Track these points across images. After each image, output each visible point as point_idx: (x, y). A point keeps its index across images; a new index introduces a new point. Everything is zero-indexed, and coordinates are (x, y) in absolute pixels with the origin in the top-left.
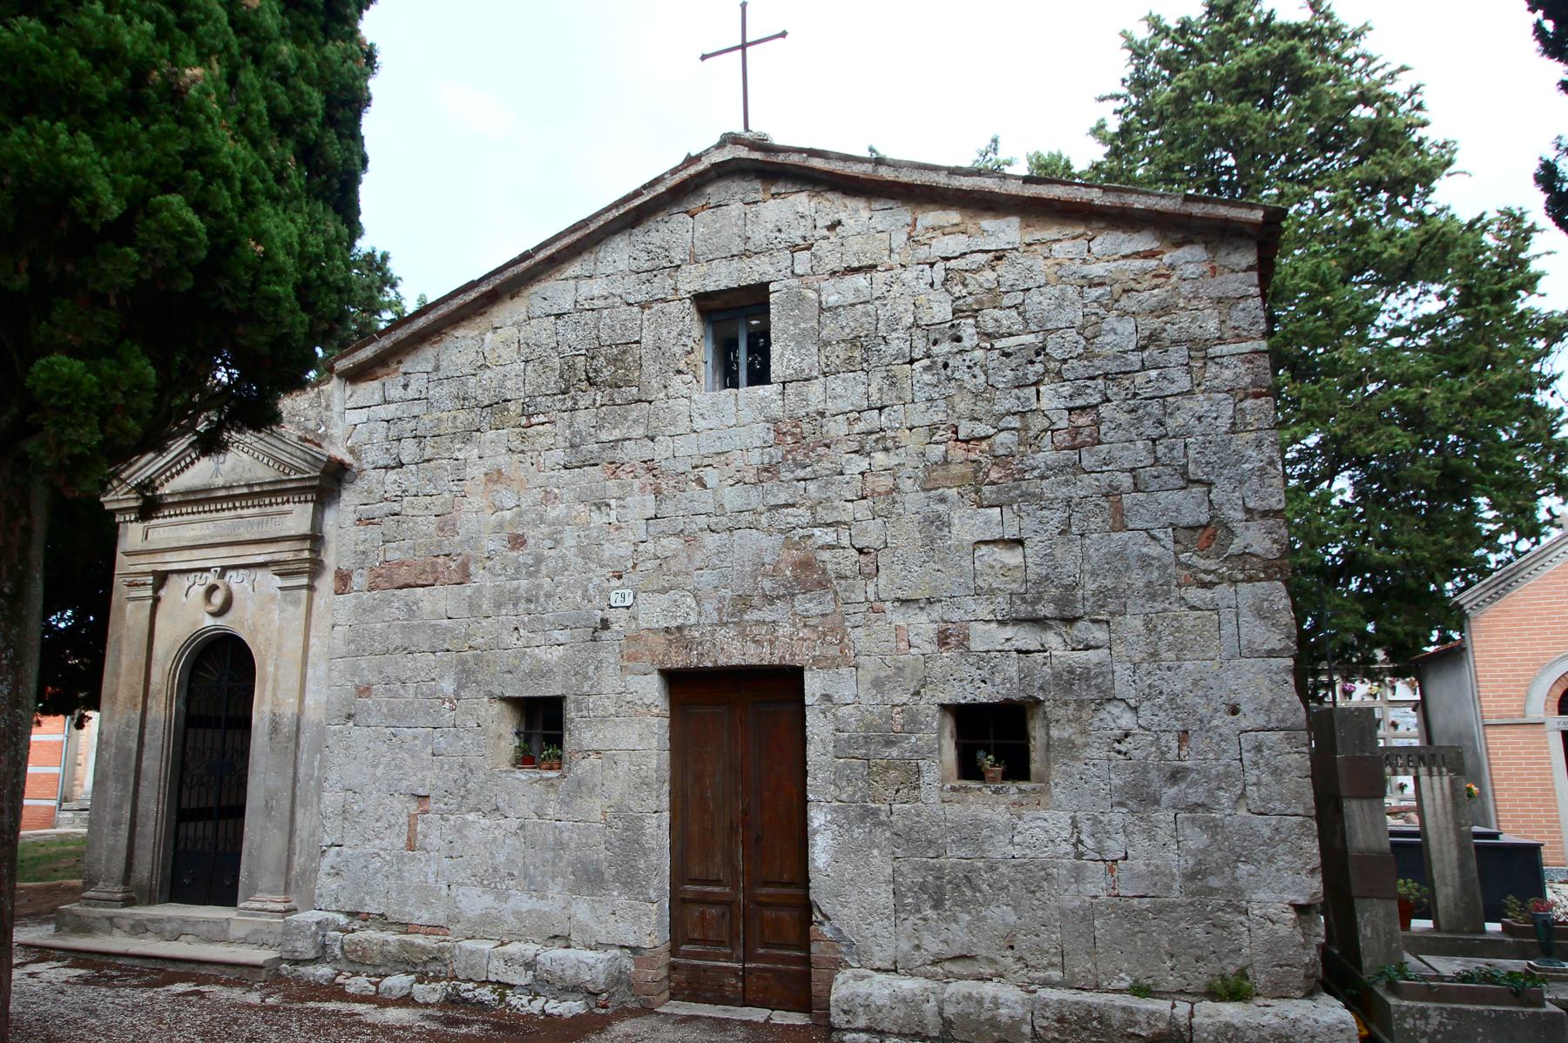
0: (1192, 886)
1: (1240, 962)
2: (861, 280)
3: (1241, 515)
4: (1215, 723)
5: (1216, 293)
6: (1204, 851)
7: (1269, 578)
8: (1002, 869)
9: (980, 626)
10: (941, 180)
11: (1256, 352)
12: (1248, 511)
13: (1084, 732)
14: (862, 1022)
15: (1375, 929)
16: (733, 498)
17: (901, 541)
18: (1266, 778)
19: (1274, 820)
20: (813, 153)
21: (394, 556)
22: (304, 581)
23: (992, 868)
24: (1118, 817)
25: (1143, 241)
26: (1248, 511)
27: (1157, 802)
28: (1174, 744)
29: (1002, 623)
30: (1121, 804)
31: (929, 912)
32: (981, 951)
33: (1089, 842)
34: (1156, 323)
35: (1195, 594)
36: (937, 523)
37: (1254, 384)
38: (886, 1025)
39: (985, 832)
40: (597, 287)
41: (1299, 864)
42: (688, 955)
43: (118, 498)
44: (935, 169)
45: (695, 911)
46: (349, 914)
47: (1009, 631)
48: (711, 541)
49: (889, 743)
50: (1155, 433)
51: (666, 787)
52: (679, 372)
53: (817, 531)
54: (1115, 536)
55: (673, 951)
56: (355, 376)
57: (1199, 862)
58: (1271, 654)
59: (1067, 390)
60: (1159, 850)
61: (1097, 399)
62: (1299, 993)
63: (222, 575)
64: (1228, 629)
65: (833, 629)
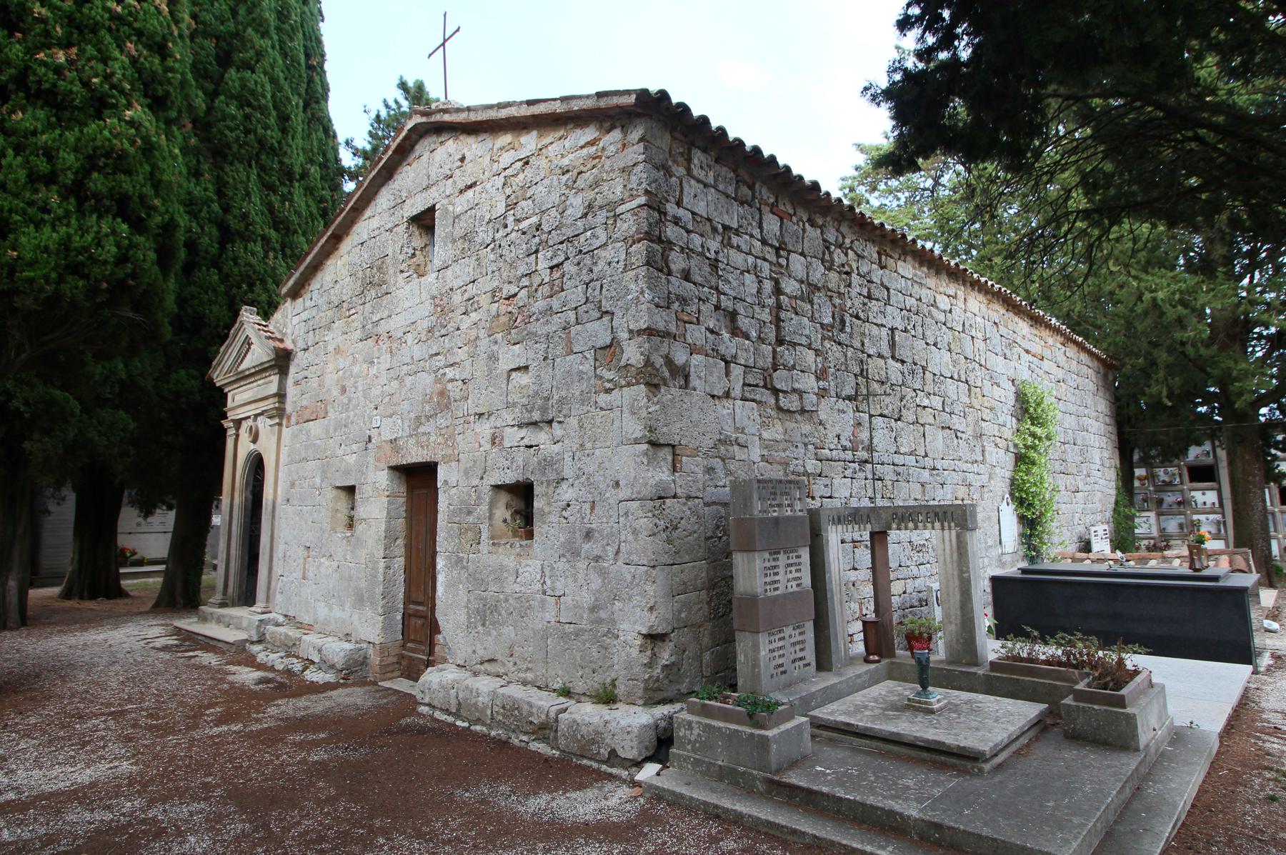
0: (593, 617)
1: (613, 675)
2: (470, 193)
3: (626, 335)
4: (608, 495)
5: (622, 165)
6: (598, 591)
7: (638, 383)
8: (511, 601)
9: (508, 430)
10: (493, 114)
11: (640, 206)
12: (631, 331)
13: (549, 504)
14: (427, 700)
15: (746, 656)
16: (418, 351)
17: (478, 374)
18: (630, 537)
19: (632, 569)
20: (501, 106)
21: (304, 403)
22: (277, 420)
23: (507, 600)
24: (561, 565)
25: (589, 133)
26: (631, 331)
27: (579, 555)
28: (588, 511)
29: (520, 426)
30: (563, 555)
31: (480, 628)
32: (499, 657)
33: (548, 582)
34: (591, 195)
35: (603, 399)
36: (493, 358)
37: (638, 232)
38: (435, 703)
39: (505, 574)
40: (375, 223)
41: (643, 604)
42: (413, 650)
43: (219, 377)
44: (509, 105)
45: (413, 620)
46: (286, 616)
47: (523, 432)
48: (409, 380)
49: (469, 513)
50: (587, 279)
51: (400, 542)
52: (402, 271)
53: (447, 370)
54: (568, 358)
55: (403, 646)
56: (295, 294)
57: (596, 600)
58: (637, 442)
59: (549, 254)
60: (579, 589)
61: (561, 259)
62: (641, 702)
63: (255, 420)
64: (617, 424)
65: (449, 437)
